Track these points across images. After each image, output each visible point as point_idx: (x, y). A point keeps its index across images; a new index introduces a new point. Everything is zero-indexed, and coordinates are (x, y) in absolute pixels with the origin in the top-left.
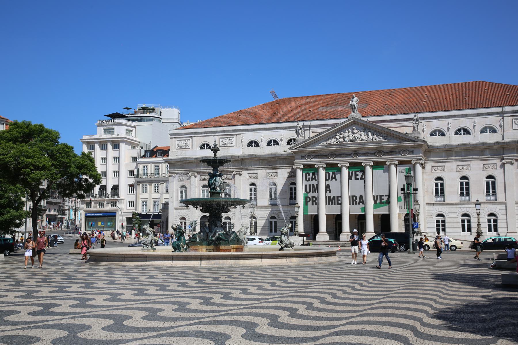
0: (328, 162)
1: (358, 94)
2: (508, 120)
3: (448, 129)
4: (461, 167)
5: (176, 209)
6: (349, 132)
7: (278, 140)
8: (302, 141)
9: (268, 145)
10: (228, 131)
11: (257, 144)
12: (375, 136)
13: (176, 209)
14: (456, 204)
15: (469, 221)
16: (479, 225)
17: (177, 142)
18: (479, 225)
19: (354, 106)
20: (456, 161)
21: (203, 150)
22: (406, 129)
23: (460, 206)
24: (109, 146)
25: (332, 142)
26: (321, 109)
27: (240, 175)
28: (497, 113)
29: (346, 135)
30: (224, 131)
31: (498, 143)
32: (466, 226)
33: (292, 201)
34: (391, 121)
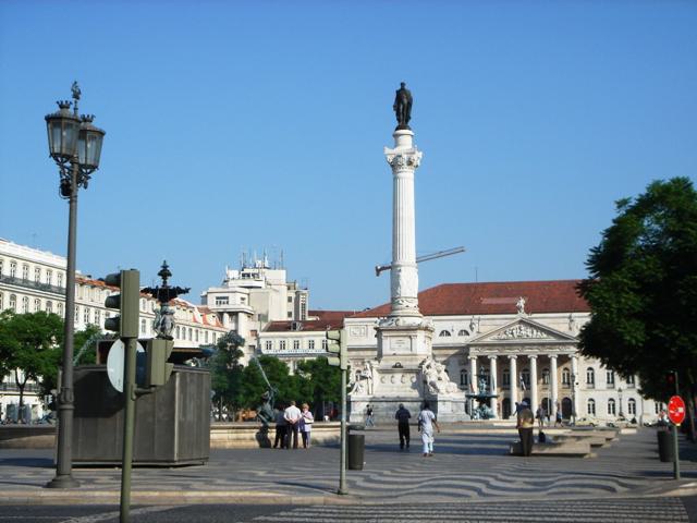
15: (614, 405)
16: (621, 408)
18: (621, 408)
24: (226, 316)
26: (486, 301)
32: (612, 409)
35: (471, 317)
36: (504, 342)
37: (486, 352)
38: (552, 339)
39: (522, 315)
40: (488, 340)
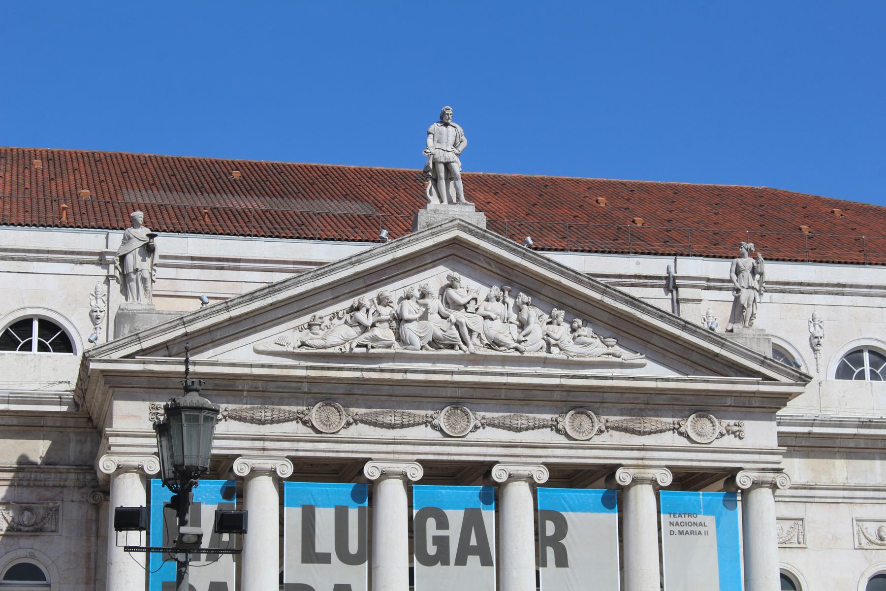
3: (815, 344)
4: (871, 529)
6: (423, 296)
12: (562, 331)
19: (447, 165)
20: (850, 501)
22: (708, 310)
25: (329, 342)
29: (410, 310)
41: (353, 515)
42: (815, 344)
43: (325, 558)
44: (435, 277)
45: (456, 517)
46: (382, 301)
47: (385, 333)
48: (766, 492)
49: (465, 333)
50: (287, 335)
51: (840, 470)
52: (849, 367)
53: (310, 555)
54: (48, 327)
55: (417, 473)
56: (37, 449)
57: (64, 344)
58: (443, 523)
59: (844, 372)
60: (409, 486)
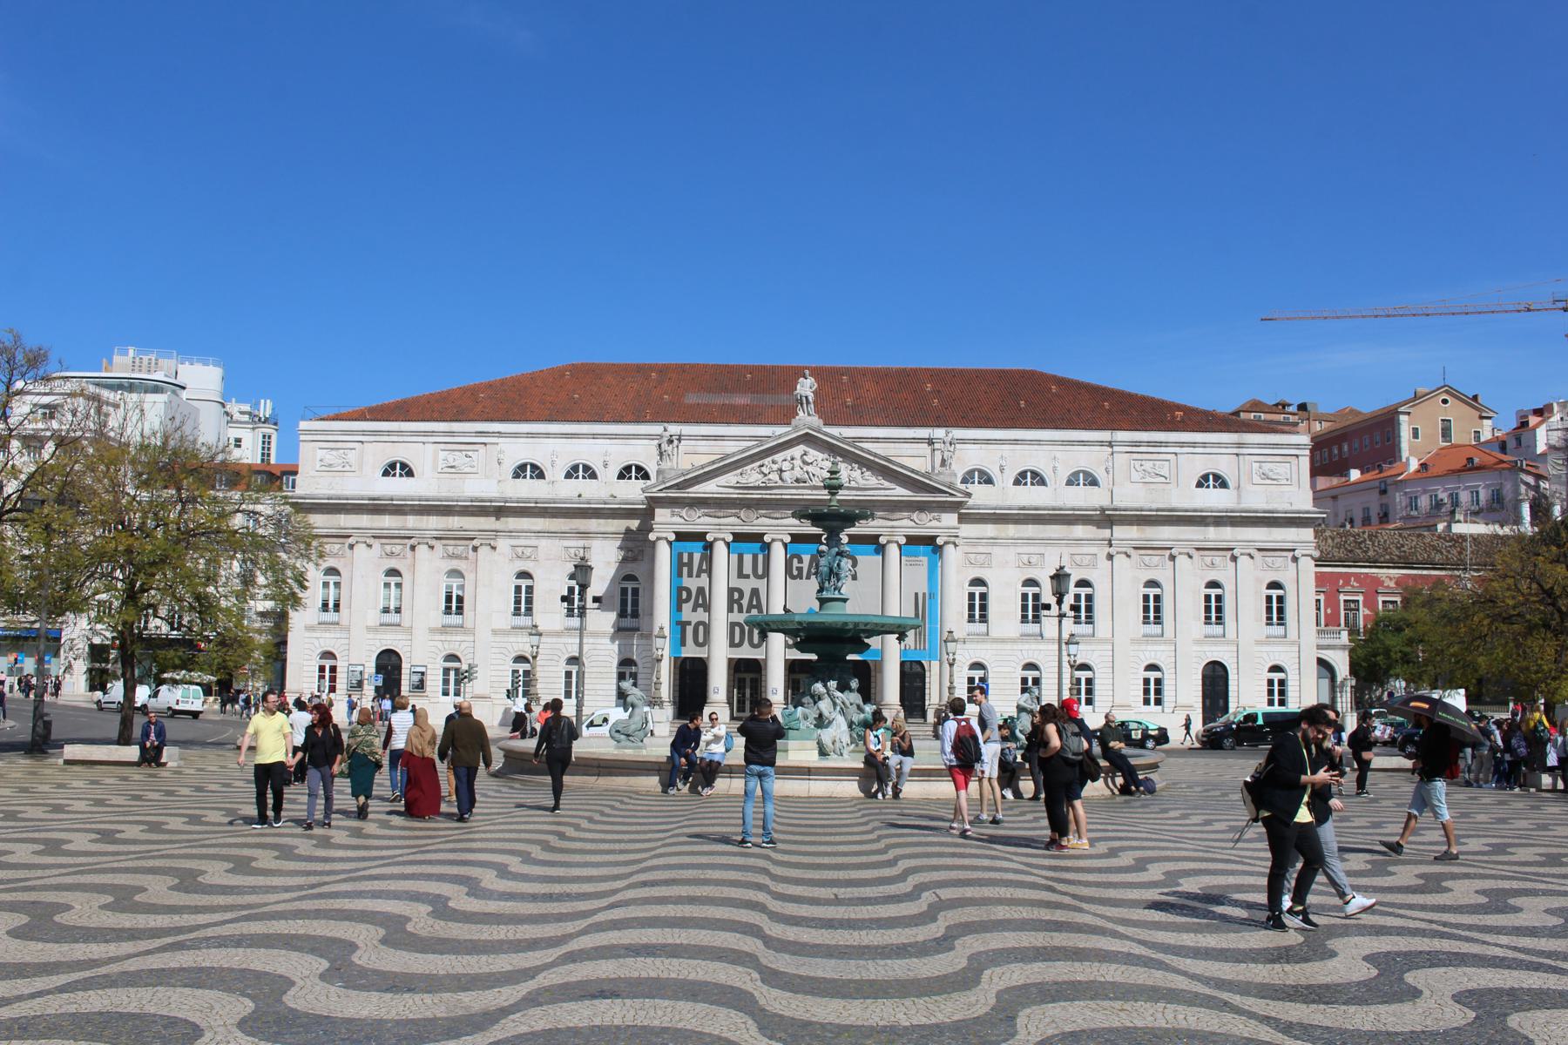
0: (738, 529)
1: (818, 373)
2: (1121, 459)
4: (1025, 558)
5: (309, 628)
7: (597, 467)
8: (673, 473)
9: (568, 476)
10: (464, 434)
11: (538, 473)
12: (857, 474)
13: (309, 628)
14: (1013, 641)
17: (320, 454)
21: (390, 479)
23: (1020, 646)
26: (691, 399)
27: (494, 548)
28: (1101, 443)
30: (451, 433)
31: (1103, 510)
33: (628, 622)
34: (876, 440)
35: (657, 429)
36: (756, 495)
37: (698, 521)
38: (900, 493)
39: (807, 419)
40: (709, 488)
41: (760, 557)
42: (1002, 470)
43: (747, 577)
44: (797, 451)
45: (806, 558)
46: (774, 462)
47: (774, 477)
48: (951, 546)
49: (811, 476)
50: (731, 478)
51: (1012, 530)
52: (1020, 479)
53: (741, 575)
54: (639, 469)
55: (788, 539)
56: (634, 524)
57: (646, 476)
58: (801, 561)
59: (1017, 482)
60: (785, 545)
